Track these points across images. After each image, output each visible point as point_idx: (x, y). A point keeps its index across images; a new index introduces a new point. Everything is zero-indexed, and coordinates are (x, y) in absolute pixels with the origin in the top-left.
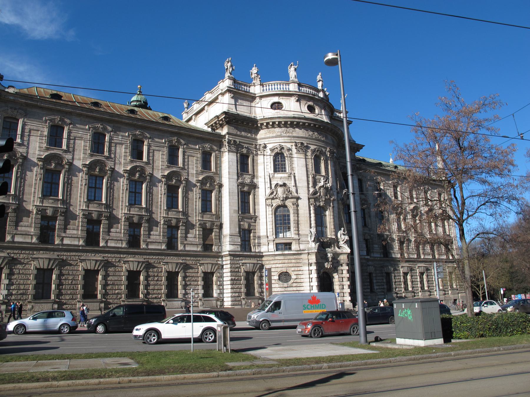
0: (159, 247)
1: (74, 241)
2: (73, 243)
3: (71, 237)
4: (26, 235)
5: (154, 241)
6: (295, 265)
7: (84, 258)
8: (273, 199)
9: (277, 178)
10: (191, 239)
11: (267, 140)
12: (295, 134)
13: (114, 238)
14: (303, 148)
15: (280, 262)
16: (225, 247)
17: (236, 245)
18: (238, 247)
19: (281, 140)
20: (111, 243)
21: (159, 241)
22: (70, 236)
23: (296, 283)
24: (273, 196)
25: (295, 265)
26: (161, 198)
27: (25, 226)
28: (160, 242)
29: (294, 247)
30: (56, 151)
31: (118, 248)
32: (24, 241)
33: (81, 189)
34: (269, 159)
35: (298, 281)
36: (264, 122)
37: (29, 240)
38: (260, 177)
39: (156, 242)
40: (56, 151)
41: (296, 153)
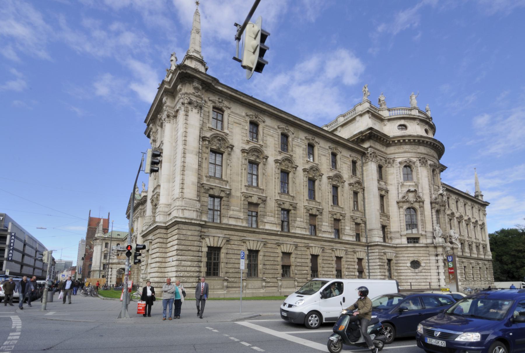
0: (330, 236)
2: (272, 229)
3: (271, 223)
4: (238, 218)
6: (424, 255)
7: (281, 242)
8: (404, 202)
9: (406, 185)
11: (397, 155)
12: (419, 151)
13: (300, 227)
14: (423, 162)
15: (412, 252)
19: (408, 155)
20: (298, 230)
22: (270, 222)
23: (425, 269)
24: (404, 199)
26: (328, 195)
27: (236, 211)
28: (330, 232)
32: (236, 224)
33: (275, 182)
34: (399, 171)
35: (426, 268)
36: (396, 139)
39: (327, 232)
41: (420, 166)
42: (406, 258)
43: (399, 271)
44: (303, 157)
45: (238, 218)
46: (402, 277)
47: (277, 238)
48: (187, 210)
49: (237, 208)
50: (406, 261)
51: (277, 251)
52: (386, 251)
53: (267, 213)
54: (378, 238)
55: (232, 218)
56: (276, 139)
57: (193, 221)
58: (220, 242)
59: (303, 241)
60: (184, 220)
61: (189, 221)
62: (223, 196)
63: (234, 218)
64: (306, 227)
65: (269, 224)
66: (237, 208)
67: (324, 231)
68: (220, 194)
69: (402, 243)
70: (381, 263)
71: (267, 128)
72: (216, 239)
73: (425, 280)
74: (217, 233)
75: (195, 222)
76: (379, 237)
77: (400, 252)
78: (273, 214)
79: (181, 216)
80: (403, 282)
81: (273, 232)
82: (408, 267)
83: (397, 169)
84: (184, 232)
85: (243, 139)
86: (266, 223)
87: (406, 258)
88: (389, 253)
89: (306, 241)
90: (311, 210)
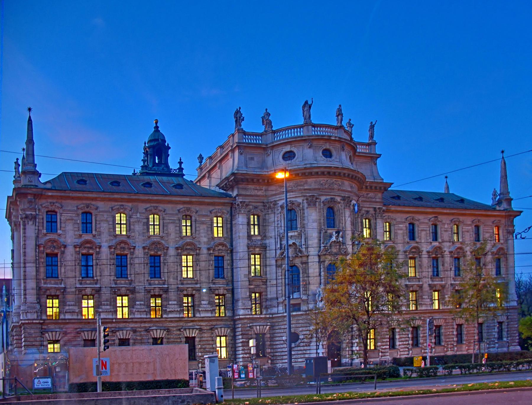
1: (109, 315)
2: (108, 317)
3: (106, 312)
5: (173, 310)
10: (205, 306)
11: (278, 196)
16: (237, 311)
17: (247, 309)
18: (248, 311)
21: (176, 309)
25: (303, 325)
29: (304, 307)
30: (87, 237)
31: (143, 318)
32: (72, 318)
37: (75, 317)
38: (271, 237)
40: (87, 237)
42: (282, 331)
43: (275, 347)
44: (143, 233)
45: (73, 312)
46: (277, 354)
47: (113, 325)
48: (29, 312)
49: (73, 303)
50: (282, 334)
51: (114, 338)
52: (254, 324)
53: (103, 302)
54: (242, 310)
55: (68, 312)
56: (111, 223)
57: (34, 321)
58: (57, 335)
59: (143, 325)
60: (27, 322)
61: (31, 321)
62: (59, 294)
63: (69, 312)
64: (147, 310)
65: (104, 313)
66: (73, 303)
67: (170, 311)
68: (56, 293)
69: (279, 312)
70: (244, 340)
71: (101, 213)
72: (54, 333)
73: (302, 356)
74: (56, 328)
75: (36, 321)
76: (243, 309)
77: (277, 324)
78: (109, 303)
79: (25, 318)
80: (278, 360)
81: (108, 320)
82: (284, 341)
83: (278, 215)
84: (28, 331)
85: (76, 234)
86: (101, 312)
87: (282, 331)
88: (258, 327)
89: (147, 325)
90: (152, 291)
